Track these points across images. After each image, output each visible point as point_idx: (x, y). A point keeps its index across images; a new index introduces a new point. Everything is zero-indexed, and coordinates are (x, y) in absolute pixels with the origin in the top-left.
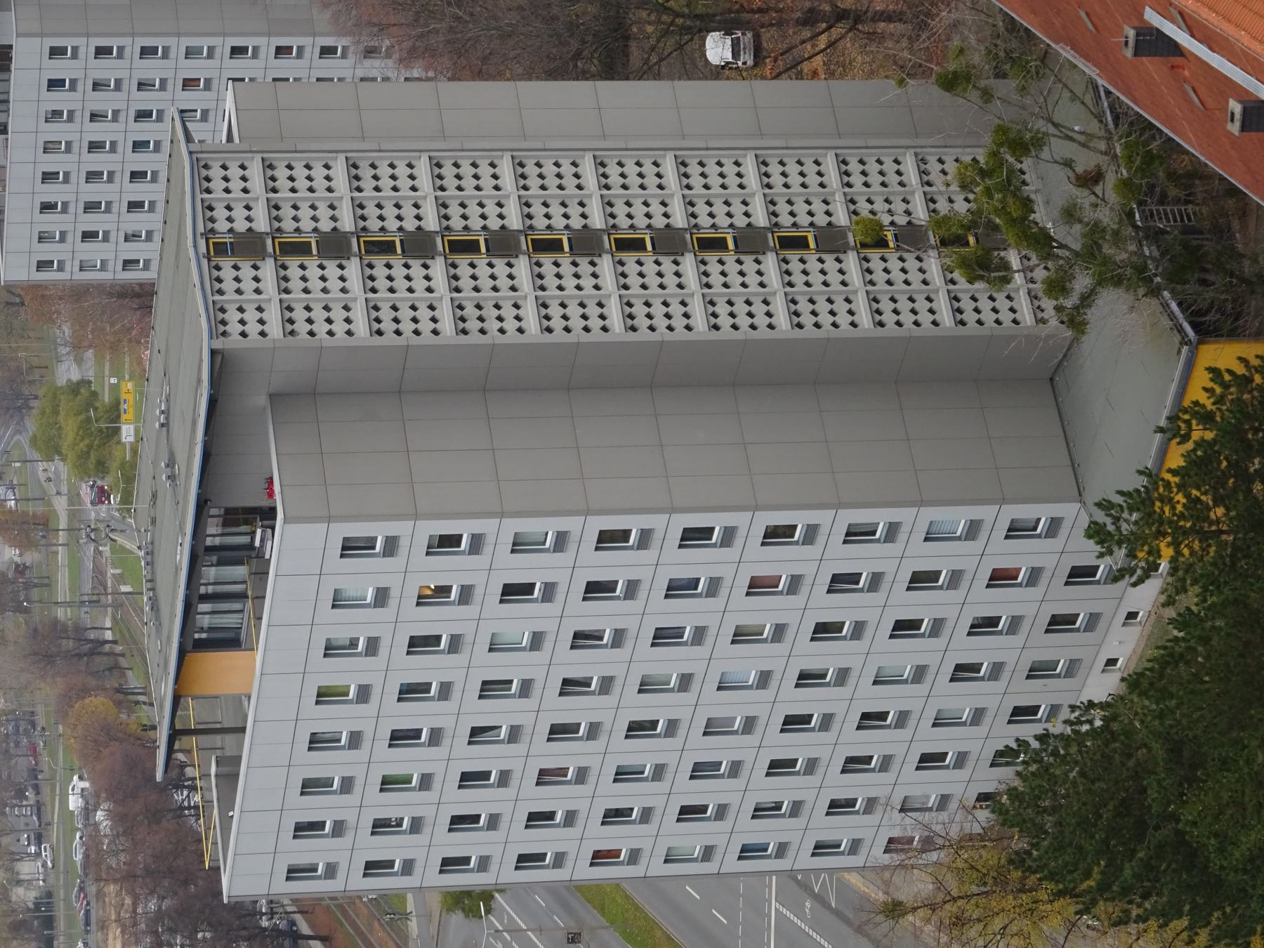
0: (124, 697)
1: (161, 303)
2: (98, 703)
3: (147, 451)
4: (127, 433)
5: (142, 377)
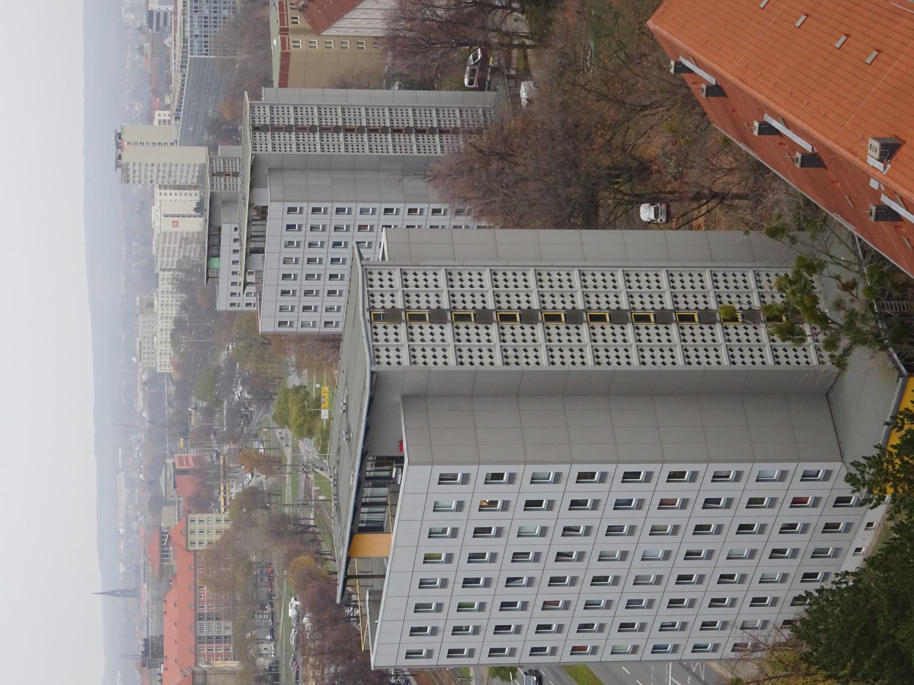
0: (320, 557)
1: (345, 346)
3: (335, 424)
4: (325, 414)
5: (333, 384)
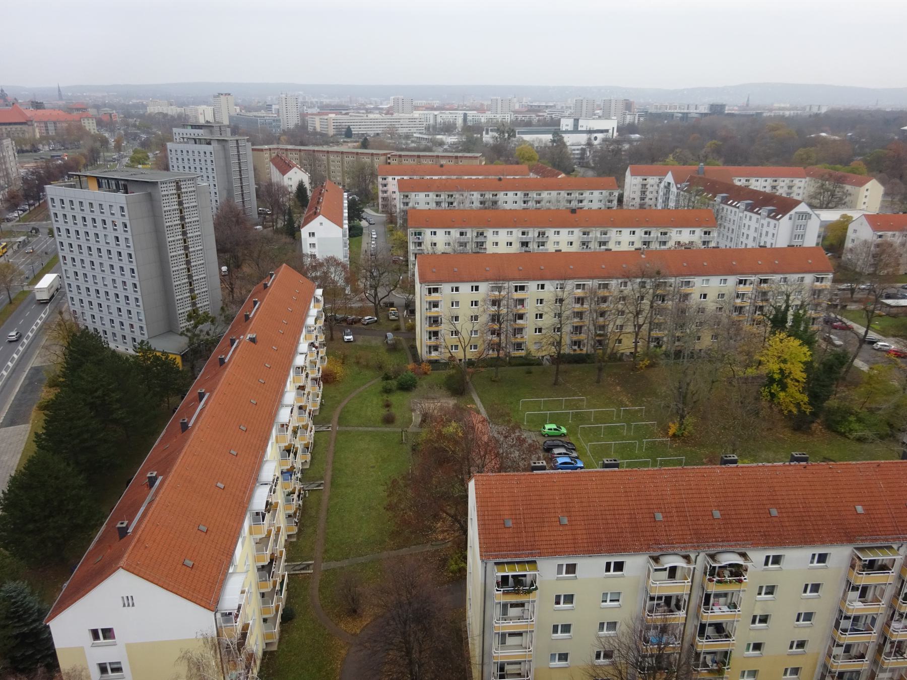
0: (86, 166)
2: (84, 161)
4: (140, 166)
5: (151, 169)
